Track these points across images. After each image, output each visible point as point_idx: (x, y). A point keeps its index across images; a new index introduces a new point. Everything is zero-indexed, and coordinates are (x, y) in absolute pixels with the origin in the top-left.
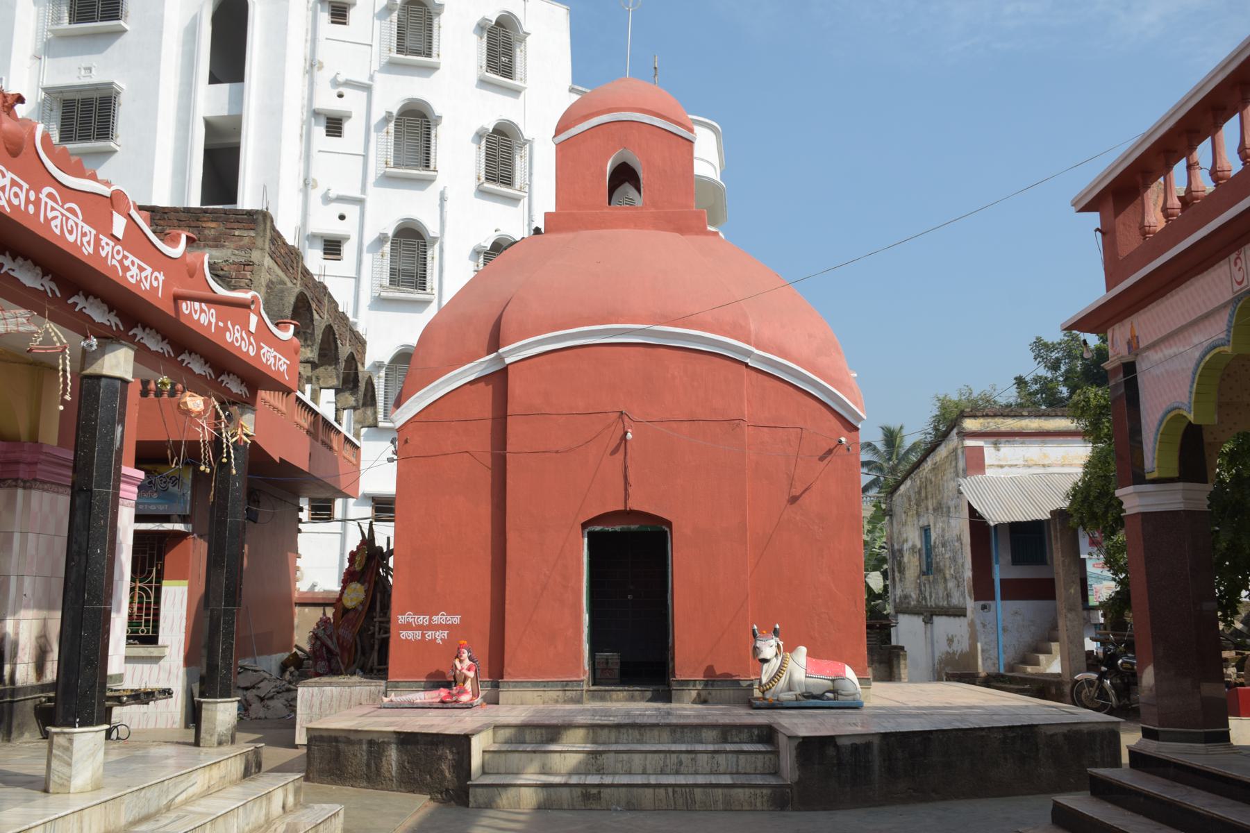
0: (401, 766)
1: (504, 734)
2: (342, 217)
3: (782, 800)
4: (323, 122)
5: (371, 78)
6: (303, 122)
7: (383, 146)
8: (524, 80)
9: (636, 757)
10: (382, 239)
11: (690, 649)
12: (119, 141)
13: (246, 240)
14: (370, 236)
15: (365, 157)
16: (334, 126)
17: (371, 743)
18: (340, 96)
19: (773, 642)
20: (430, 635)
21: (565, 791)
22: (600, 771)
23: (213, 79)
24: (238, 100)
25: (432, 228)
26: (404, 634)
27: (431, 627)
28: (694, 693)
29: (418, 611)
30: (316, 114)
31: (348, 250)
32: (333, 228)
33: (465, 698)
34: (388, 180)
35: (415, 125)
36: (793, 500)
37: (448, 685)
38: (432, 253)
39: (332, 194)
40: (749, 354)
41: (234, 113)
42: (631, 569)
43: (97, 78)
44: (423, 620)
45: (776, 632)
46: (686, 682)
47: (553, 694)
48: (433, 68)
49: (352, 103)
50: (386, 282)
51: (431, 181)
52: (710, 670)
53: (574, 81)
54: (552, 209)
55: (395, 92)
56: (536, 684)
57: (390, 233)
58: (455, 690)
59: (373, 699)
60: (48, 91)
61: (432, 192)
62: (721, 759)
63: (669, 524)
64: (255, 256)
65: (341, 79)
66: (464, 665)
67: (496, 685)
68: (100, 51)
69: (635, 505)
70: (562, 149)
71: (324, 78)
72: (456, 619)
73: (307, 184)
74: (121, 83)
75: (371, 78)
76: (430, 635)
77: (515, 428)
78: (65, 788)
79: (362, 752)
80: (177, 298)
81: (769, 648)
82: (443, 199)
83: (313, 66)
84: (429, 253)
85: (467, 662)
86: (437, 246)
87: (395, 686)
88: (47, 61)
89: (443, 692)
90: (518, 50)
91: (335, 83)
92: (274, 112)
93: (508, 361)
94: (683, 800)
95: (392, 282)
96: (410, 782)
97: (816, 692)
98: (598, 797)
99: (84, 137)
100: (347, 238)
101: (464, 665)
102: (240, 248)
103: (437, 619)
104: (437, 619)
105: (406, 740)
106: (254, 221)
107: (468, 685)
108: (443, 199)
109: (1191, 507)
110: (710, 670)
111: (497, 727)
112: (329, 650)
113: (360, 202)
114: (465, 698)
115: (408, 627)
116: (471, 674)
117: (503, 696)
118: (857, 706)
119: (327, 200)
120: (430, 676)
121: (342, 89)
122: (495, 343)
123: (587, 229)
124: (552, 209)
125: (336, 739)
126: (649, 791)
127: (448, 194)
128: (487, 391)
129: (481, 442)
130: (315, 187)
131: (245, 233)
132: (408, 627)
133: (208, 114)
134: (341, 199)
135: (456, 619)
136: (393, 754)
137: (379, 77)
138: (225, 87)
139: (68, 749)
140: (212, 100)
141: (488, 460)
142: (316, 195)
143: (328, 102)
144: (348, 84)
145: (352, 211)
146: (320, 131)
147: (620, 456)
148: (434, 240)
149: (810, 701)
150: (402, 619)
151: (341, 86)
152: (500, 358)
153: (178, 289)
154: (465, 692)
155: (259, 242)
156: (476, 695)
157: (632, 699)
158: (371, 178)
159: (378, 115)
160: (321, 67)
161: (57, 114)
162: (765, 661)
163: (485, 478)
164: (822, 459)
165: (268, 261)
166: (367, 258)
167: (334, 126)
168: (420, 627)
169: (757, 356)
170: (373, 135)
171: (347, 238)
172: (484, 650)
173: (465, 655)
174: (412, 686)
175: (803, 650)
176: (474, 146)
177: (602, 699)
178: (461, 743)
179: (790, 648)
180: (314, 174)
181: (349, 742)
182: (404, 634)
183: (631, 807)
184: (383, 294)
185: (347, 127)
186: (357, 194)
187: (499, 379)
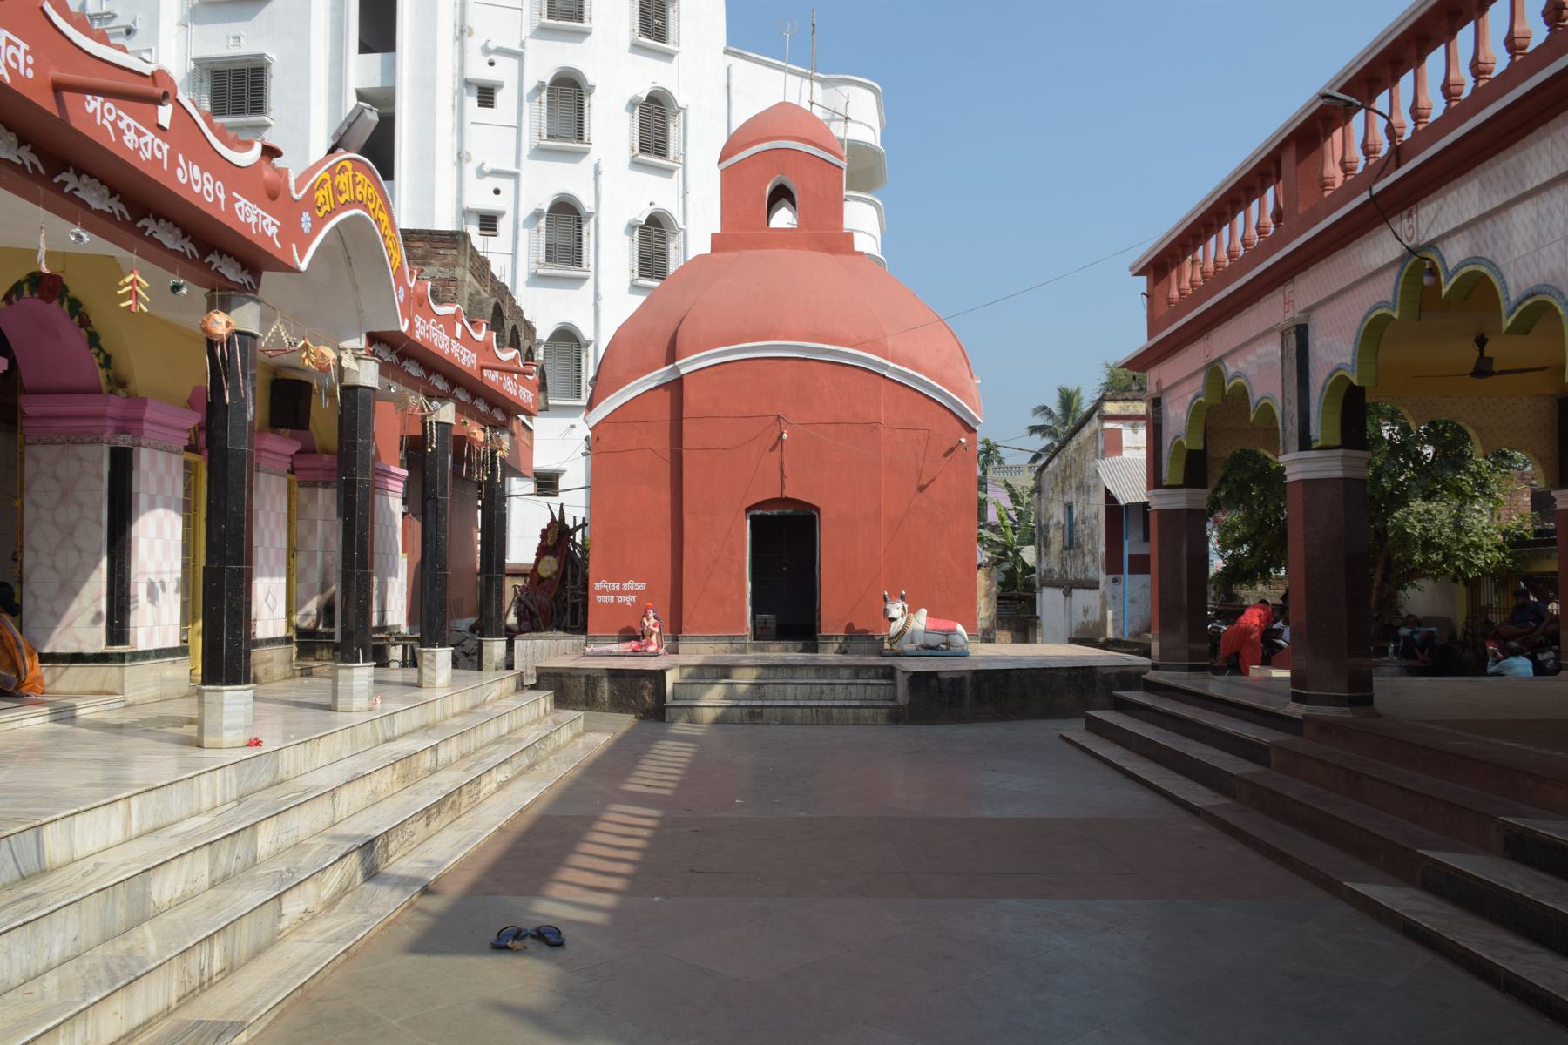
0: (612, 695)
1: (686, 671)
2: (497, 192)
3: (897, 717)
4: (475, 91)
5: (523, 44)
6: (455, 92)
7: (536, 116)
8: (677, 43)
9: (789, 688)
10: (537, 215)
11: (833, 611)
12: (272, 114)
13: (450, 259)
14: (525, 212)
15: (519, 128)
16: (486, 96)
17: (587, 677)
18: (491, 64)
19: (900, 605)
20: (621, 598)
21: (737, 710)
22: (761, 698)
23: (365, 48)
24: (390, 70)
25: (587, 204)
26: (599, 598)
27: (622, 592)
28: (836, 646)
29: (610, 580)
30: (468, 83)
31: (504, 225)
32: (490, 204)
33: (652, 648)
34: (541, 152)
35: (568, 93)
36: (921, 489)
37: (637, 638)
38: (588, 228)
39: (487, 168)
40: (885, 367)
41: (387, 84)
42: (786, 547)
43: (246, 48)
44: (615, 586)
45: (902, 598)
46: (830, 637)
47: (723, 646)
48: (585, 34)
49: (502, 73)
50: (543, 258)
51: (585, 153)
52: (850, 627)
53: (729, 42)
54: (718, 230)
55: (547, 60)
56: (708, 638)
57: (546, 210)
58: (643, 642)
59: (575, 649)
60: (195, 60)
61: (587, 164)
62: (853, 689)
63: (818, 509)
64: (458, 272)
65: (492, 46)
66: (650, 622)
67: (676, 639)
68: (249, 19)
69: (788, 494)
70: (726, 174)
71: (474, 44)
72: (642, 586)
73: (461, 157)
74: (272, 55)
75: (523, 44)
76: (621, 598)
77: (689, 428)
78: (432, 685)
79: (581, 685)
80: (482, 368)
81: (896, 610)
82: (597, 172)
83: (463, 32)
84: (585, 229)
85: (653, 621)
86: (592, 221)
87: (594, 639)
88: (194, 28)
89: (634, 644)
90: (671, 11)
91: (486, 50)
92: (427, 85)
93: (683, 371)
94: (824, 716)
95: (549, 259)
96: (618, 704)
97: (932, 644)
98: (761, 715)
99: (238, 111)
100: (502, 214)
101: (650, 622)
102: (445, 266)
103: (626, 586)
104: (626, 586)
105: (615, 674)
106: (456, 241)
107: (654, 638)
108: (597, 172)
109: (1194, 506)
110: (850, 627)
111: (682, 667)
112: (531, 612)
113: (514, 176)
114: (652, 648)
115: (603, 592)
116: (657, 630)
117: (682, 648)
118: (964, 655)
119: (481, 174)
120: (622, 631)
121: (493, 57)
122: (672, 356)
123: (749, 248)
124: (718, 230)
125: (560, 675)
126: (798, 711)
127: (603, 167)
128: (666, 396)
129: (662, 440)
130: (468, 160)
131: (449, 252)
132: (603, 592)
133: (361, 86)
134: (496, 173)
135: (642, 586)
136: (605, 686)
137: (530, 43)
138: (375, 58)
139: (433, 661)
140: (364, 70)
141: (668, 455)
142: (470, 170)
143: (479, 71)
144: (500, 51)
145: (506, 185)
146: (472, 101)
147: (777, 452)
148: (590, 215)
149: (928, 650)
150: (598, 586)
151: (493, 54)
152: (676, 369)
153: (483, 363)
154: (650, 643)
155: (461, 260)
156: (660, 646)
157: (787, 650)
158: (525, 151)
159: (529, 86)
160: (470, 34)
161: (207, 85)
162: (893, 620)
163: (665, 470)
164: (945, 455)
165: (469, 277)
166: (524, 233)
167: (486, 96)
168: (613, 593)
169: (892, 369)
170: (526, 104)
171: (502, 214)
172: (666, 611)
173: (651, 614)
174: (609, 639)
175: (924, 611)
176: (628, 115)
177: (762, 650)
178: (660, 675)
179: (913, 610)
180: (467, 148)
181: (570, 676)
182: (599, 598)
183: (786, 721)
184: (541, 271)
185: (499, 97)
186: (511, 168)
187: (676, 386)
